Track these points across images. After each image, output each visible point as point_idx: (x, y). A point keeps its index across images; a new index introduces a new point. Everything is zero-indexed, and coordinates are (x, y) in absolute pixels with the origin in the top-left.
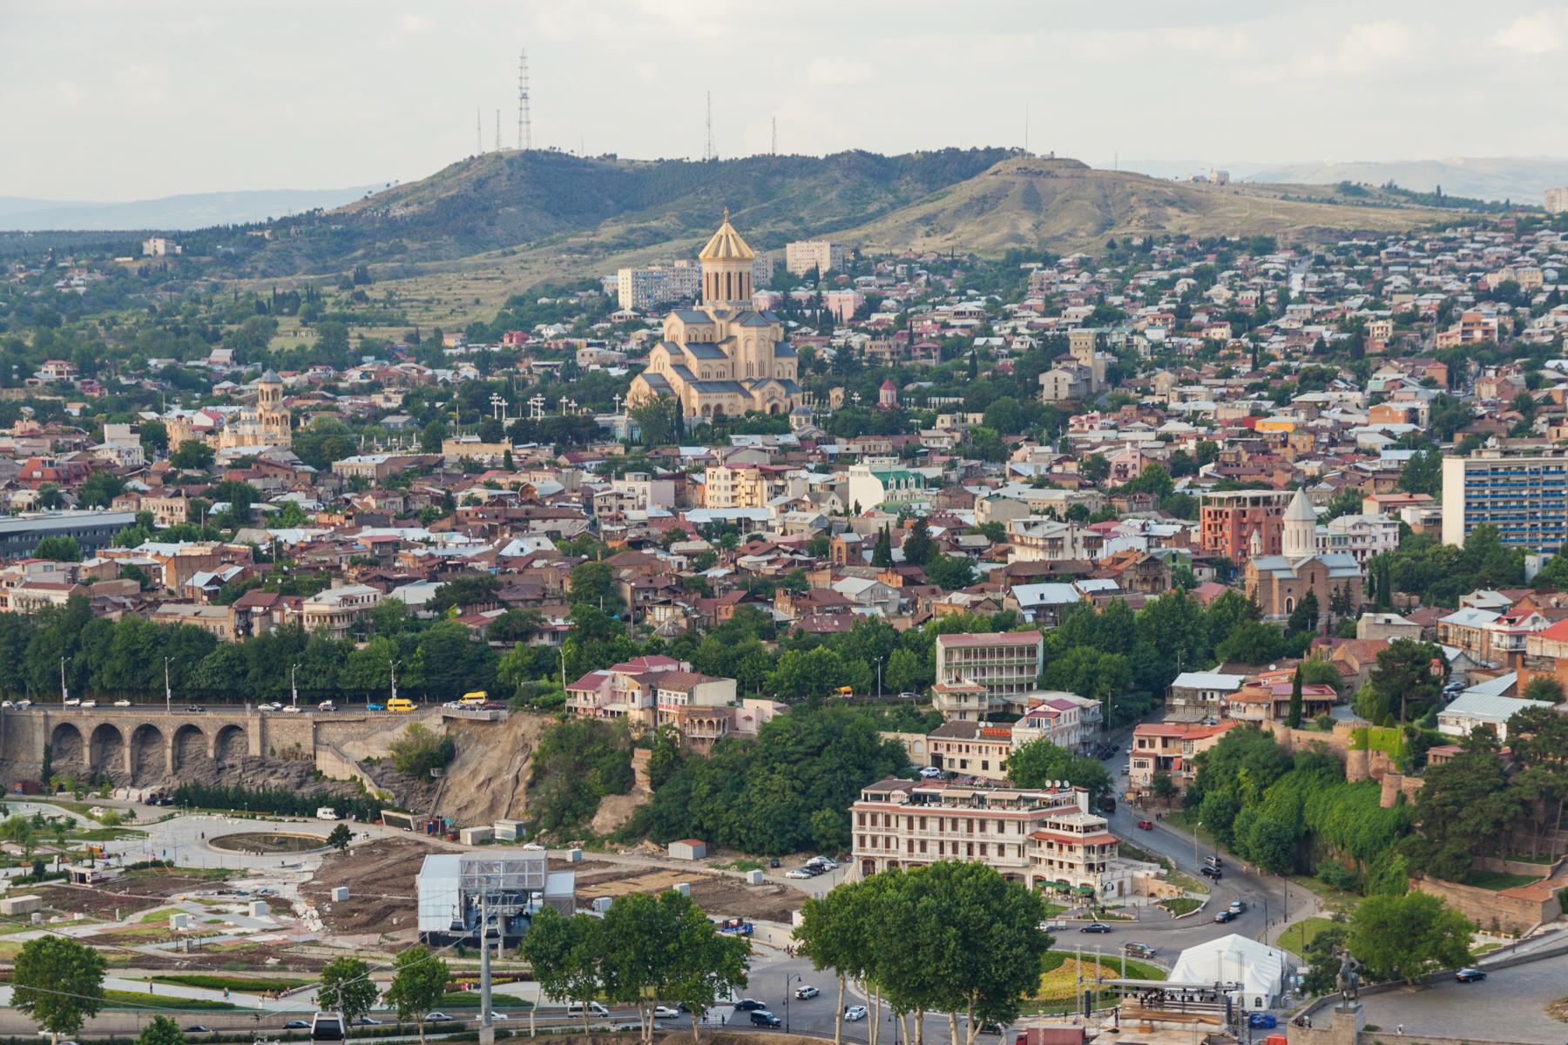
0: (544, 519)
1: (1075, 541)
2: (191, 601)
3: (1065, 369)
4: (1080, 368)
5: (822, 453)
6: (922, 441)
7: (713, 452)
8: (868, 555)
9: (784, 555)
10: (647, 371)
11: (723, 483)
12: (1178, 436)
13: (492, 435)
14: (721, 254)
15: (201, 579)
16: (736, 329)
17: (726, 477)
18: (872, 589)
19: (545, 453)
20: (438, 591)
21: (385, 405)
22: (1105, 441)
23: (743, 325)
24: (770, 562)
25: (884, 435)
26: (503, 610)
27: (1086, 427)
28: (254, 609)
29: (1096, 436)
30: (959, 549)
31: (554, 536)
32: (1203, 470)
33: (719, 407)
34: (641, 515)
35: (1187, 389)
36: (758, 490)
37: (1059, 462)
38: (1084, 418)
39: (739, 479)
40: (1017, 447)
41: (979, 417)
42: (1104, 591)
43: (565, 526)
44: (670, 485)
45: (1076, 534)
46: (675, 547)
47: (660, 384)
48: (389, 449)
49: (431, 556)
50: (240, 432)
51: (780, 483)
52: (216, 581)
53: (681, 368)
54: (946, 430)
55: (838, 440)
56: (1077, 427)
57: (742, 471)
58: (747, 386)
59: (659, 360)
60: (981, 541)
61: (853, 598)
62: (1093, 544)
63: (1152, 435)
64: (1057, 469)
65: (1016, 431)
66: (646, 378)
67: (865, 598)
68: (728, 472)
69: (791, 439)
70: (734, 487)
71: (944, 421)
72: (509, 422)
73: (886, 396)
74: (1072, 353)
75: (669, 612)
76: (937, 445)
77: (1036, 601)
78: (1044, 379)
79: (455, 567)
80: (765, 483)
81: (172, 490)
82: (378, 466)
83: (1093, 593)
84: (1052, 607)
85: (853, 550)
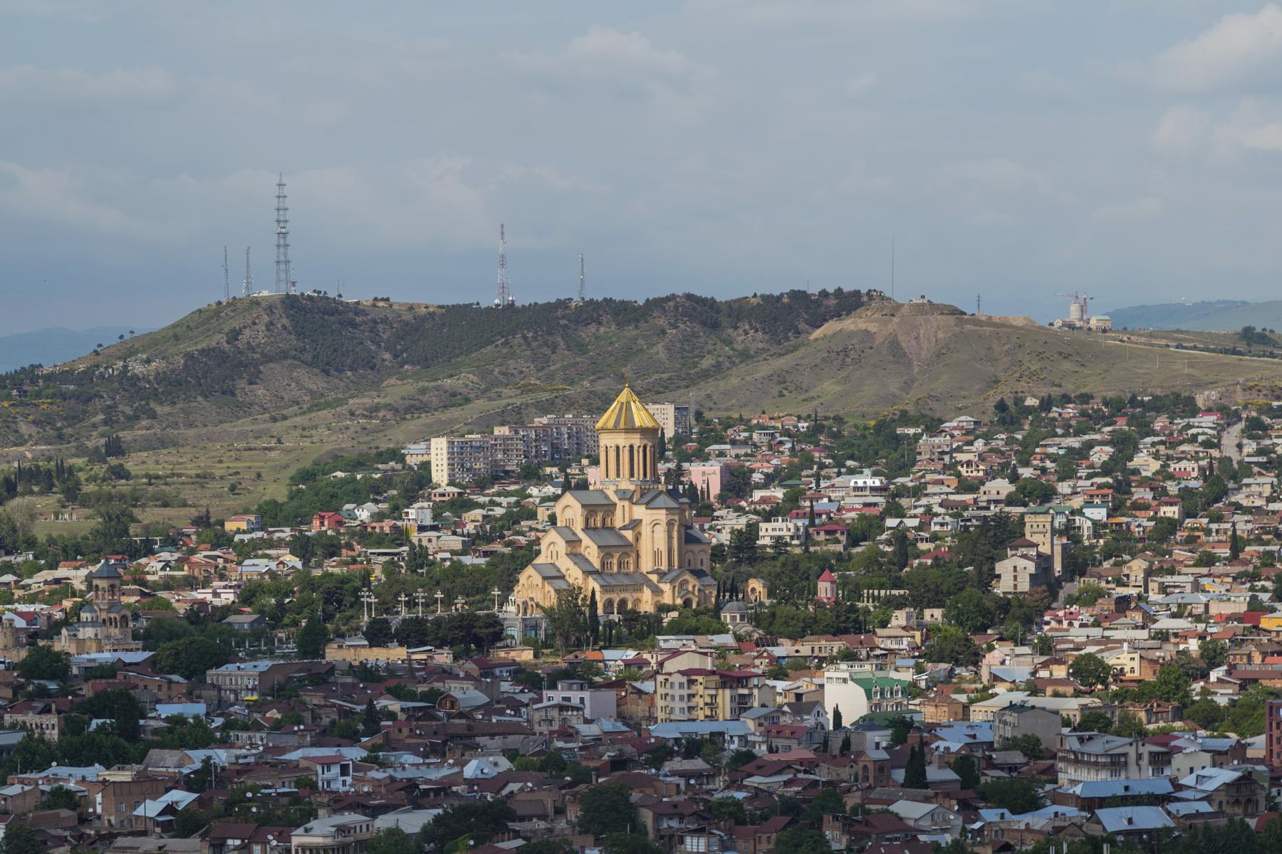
0: (492, 736)
1: (1139, 757)
2: (144, 833)
3: (1024, 556)
4: (1039, 555)
5: (770, 656)
6: (878, 641)
7: (646, 656)
8: (900, 775)
9: (801, 776)
10: (539, 560)
11: (677, 692)
12: (1176, 635)
13: (378, 635)
14: (622, 426)
15: (151, 808)
16: (640, 512)
17: (681, 685)
18: (932, 813)
19: (444, 657)
20: (437, 819)
21: (217, 602)
22: (1091, 641)
23: (648, 505)
24: (787, 783)
25: (834, 635)
26: (520, 842)
27: (1065, 623)
28: (230, 842)
29: (1078, 634)
30: (996, 767)
31: (511, 754)
32: (1214, 675)
33: (623, 602)
34: (594, 730)
35: (1168, 579)
36: (719, 700)
37: (1045, 665)
38: (1061, 613)
39: (699, 689)
40: (991, 648)
41: (938, 613)
42: (1198, 815)
43: (514, 741)
44: (611, 695)
45: (1141, 750)
46: (668, 766)
47: (552, 576)
48: (253, 656)
49: (392, 779)
50: (81, 636)
51: (745, 691)
52: (169, 809)
53: (576, 556)
54: (904, 628)
55: (780, 640)
56: (1054, 624)
57: (700, 679)
58: (654, 578)
59: (553, 548)
60: (1017, 757)
61: (911, 823)
62: (1160, 761)
63: (1144, 634)
64: (1044, 674)
65: (982, 629)
66: (536, 568)
67: (925, 824)
68: (684, 679)
69: (727, 639)
70: (691, 696)
71: (899, 618)
72: (395, 622)
73: (824, 589)
74: (1028, 537)
75: (703, 841)
76: (895, 646)
77: (1124, 825)
78: (1003, 567)
79: (437, 792)
80: (728, 692)
81: (39, 705)
82: (261, 674)
83: (1187, 816)
84: (1140, 832)
85: (881, 769)
